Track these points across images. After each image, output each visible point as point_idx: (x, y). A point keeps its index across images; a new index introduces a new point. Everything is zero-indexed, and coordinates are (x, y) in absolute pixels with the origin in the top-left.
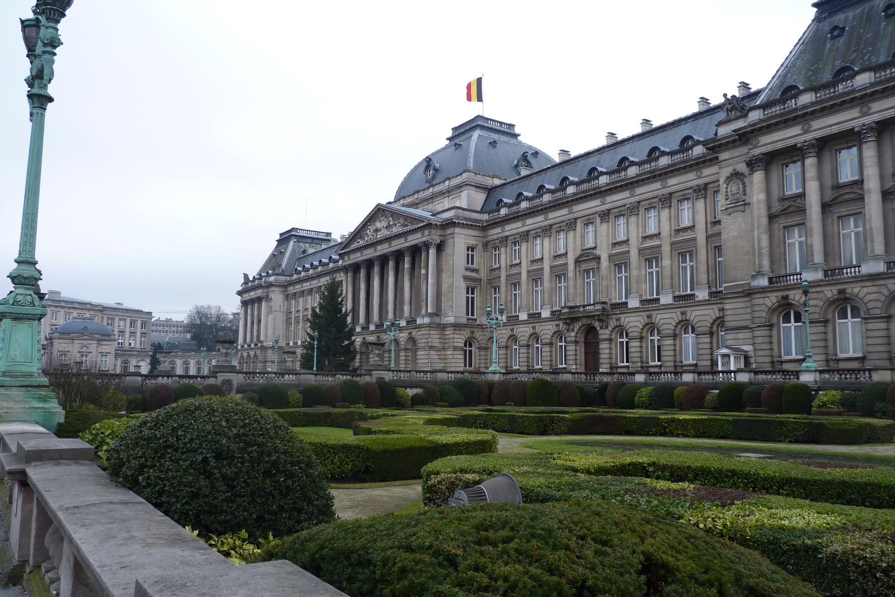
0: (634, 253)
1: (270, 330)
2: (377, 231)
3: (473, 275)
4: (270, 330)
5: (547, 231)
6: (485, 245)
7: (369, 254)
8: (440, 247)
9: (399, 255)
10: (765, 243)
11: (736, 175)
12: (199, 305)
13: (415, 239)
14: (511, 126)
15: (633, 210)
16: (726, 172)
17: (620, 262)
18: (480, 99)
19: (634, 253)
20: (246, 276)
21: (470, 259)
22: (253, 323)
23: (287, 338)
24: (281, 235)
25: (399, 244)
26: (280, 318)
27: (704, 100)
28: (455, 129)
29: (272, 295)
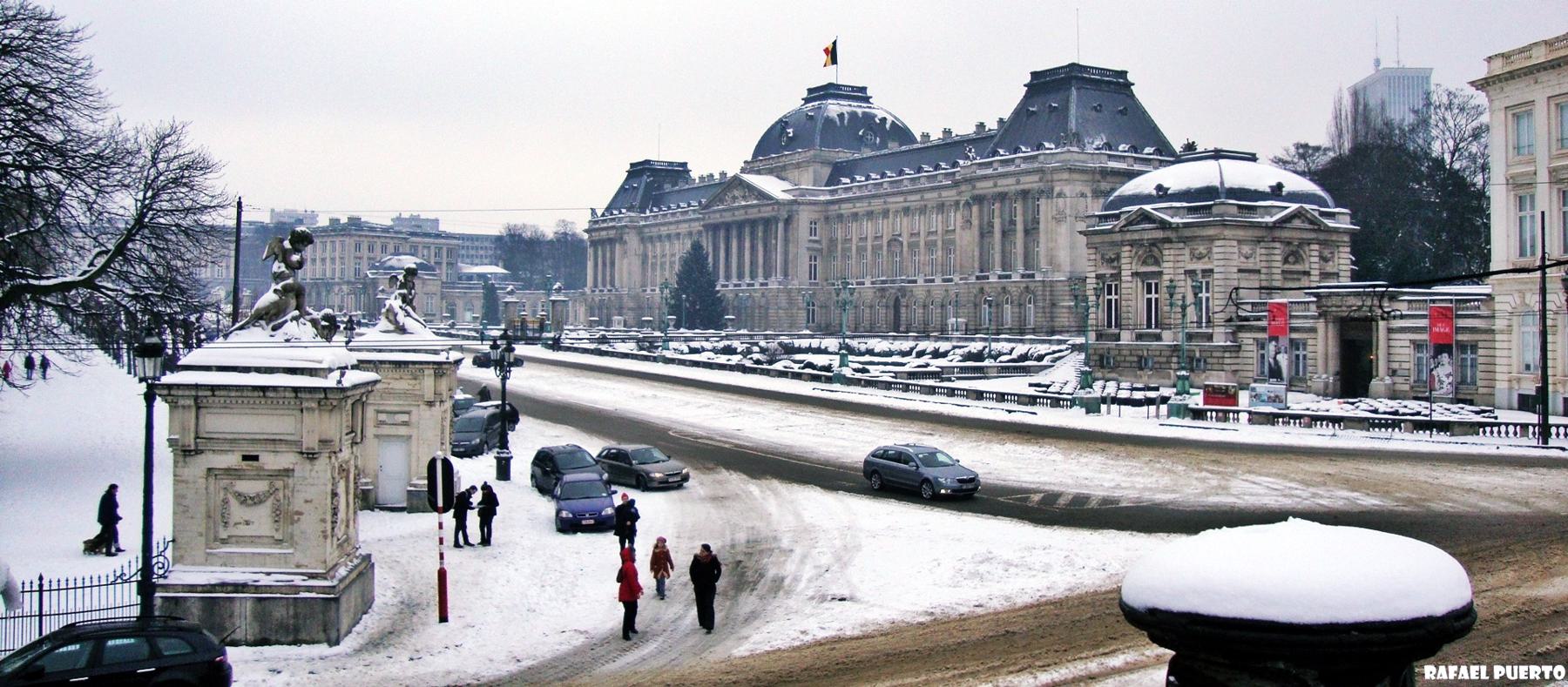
0: (922, 243)
1: (625, 275)
2: (734, 198)
3: (816, 246)
4: (625, 275)
5: (870, 215)
6: (827, 218)
7: (728, 218)
8: (788, 222)
9: (753, 223)
10: (977, 254)
11: (967, 204)
12: (512, 223)
13: (767, 212)
14: (863, 89)
15: (923, 210)
16: (963, 199)
17: (913, 246)
18: (834, 61)
19: (922, 243)
20: (593, 210)
21: (813, 232)
22: (604, 264)
23: (644, 285)
24: (632, 165)
25: (753, 214)
26: (637, 262)
27: (981, 126)
28: (810, 91)
29: (626, 237)
